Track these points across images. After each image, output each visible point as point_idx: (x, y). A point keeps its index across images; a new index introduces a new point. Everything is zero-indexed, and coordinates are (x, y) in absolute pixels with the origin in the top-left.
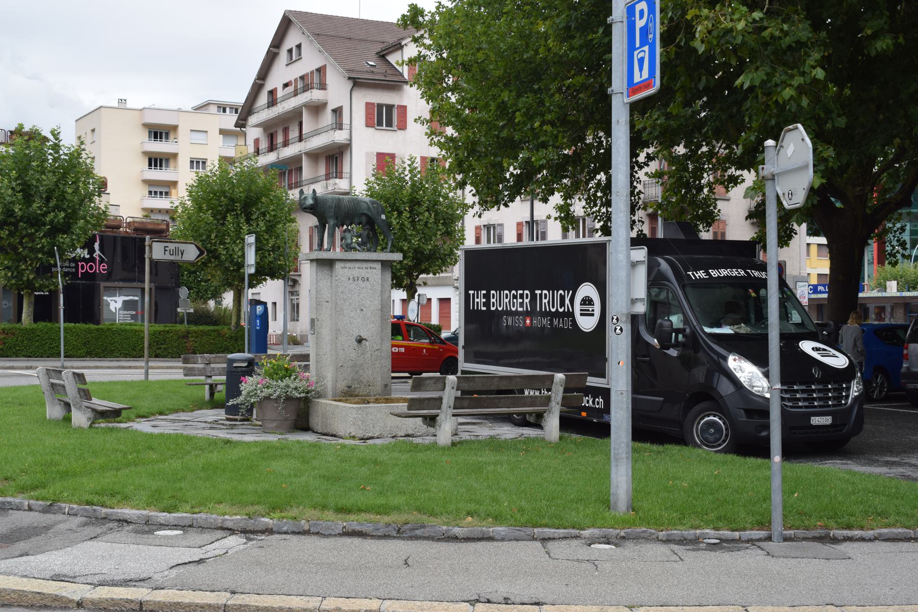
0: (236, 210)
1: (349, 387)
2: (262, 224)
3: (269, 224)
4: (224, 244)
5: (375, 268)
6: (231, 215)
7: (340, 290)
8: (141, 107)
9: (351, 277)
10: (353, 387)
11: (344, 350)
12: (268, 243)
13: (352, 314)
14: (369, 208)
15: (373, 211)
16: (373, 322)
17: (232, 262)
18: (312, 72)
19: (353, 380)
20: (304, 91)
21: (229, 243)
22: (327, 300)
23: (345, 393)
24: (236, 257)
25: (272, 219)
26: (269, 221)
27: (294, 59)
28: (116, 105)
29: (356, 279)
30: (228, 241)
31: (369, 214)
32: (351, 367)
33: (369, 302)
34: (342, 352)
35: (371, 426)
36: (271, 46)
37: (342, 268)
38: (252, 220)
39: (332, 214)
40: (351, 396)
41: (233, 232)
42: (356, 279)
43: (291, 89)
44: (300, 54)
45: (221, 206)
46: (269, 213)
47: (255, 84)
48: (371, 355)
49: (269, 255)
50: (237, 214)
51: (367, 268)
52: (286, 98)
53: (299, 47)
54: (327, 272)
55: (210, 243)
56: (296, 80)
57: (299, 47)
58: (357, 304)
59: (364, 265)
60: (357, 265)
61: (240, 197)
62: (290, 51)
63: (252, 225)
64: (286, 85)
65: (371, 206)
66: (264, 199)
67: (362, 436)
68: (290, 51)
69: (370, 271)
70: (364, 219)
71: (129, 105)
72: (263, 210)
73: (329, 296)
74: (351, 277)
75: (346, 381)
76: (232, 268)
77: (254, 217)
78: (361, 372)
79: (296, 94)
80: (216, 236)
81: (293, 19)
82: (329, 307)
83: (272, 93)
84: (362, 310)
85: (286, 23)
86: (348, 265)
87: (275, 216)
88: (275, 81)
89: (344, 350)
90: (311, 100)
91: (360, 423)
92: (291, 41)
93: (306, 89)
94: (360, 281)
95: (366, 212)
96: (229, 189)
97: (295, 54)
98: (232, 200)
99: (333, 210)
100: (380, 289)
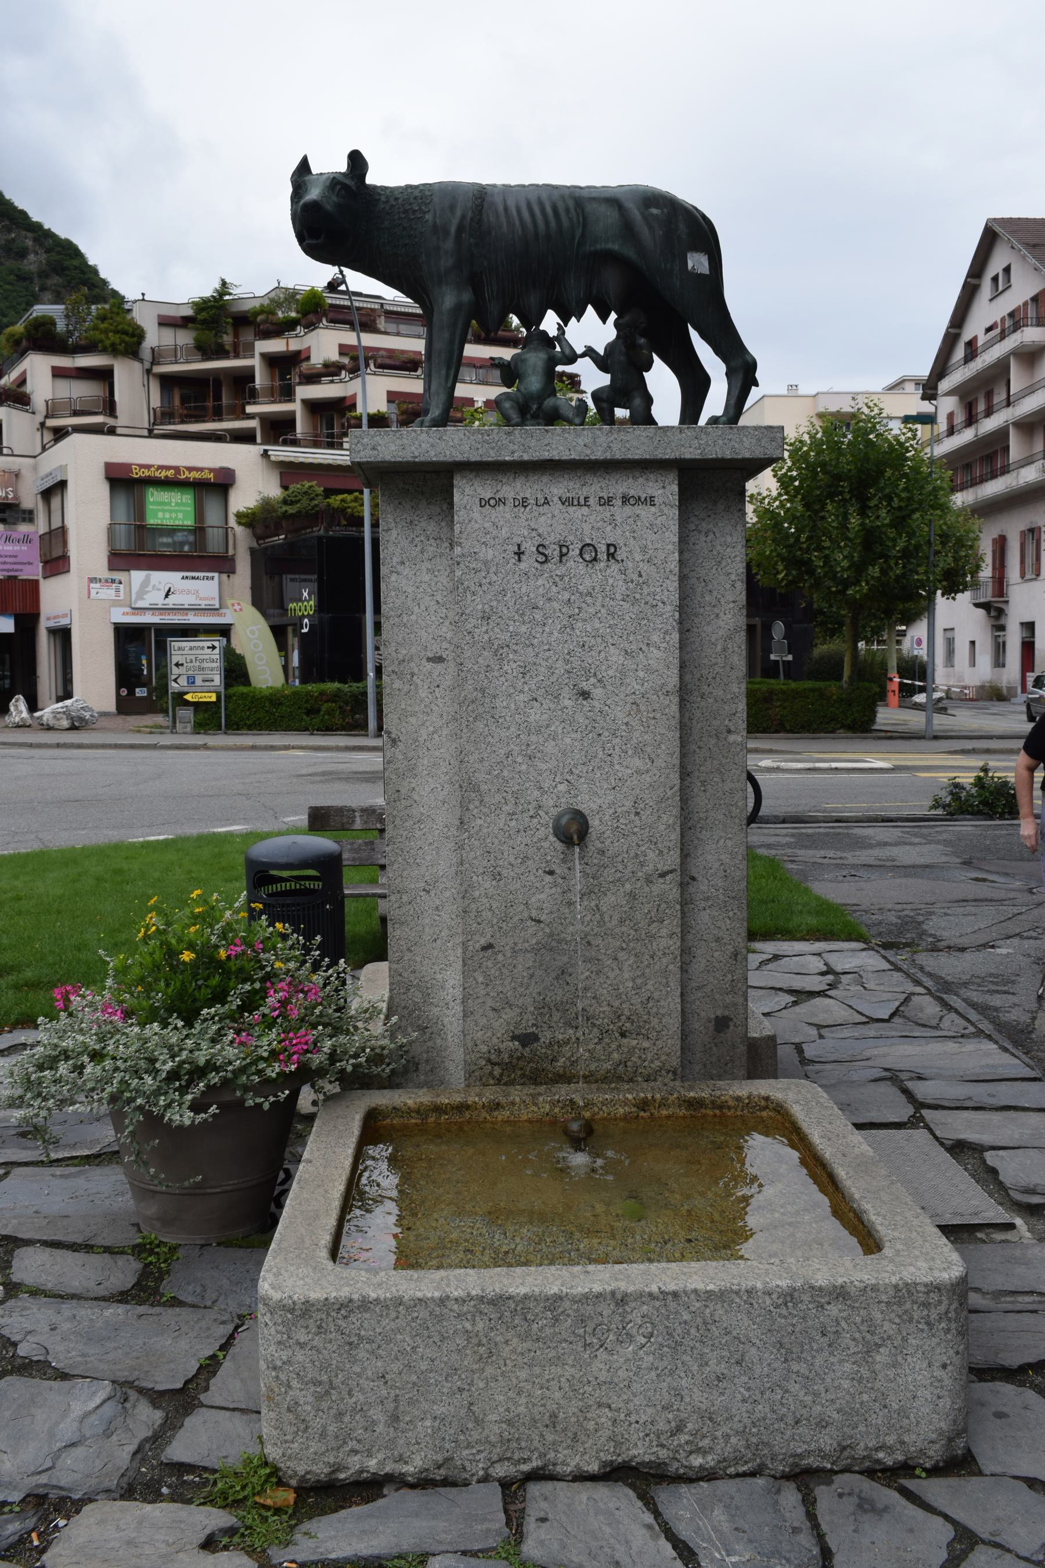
0: (841, 493)
1: (527, 1039)
2: (883, 513)
3: (898, 514)
4: (820, 548)
5: (650, 501)
6: (832, 501)
7: (477, 605)
8: (814, 393)
9: (529, 547)
10: (545, 1036)
11: (497, 876)
12: (894, 546)
13: (535, 715)
14: (627, 228)
15: (645, 233)
16: (639, 750)
17: (834, 578)
18: (1025, 304)
19: (543, 1007)
20: (1014, 331)
21: (829, 548)
22: (435, 649)
23: (509, 1067)
24: (839, 569)
25: (903, 504)
26: (900, 508)
27: (1001, 288)
28: (785, 392)
29: (553, 551)
30: (827, 544)
31: (630, 253)
32: (536, 950)
33: (616, 657)
34: (488, 884)
35: (377, 1414)
36: (968, 276)
37: (483, 503)
38: (870, 507)
39: (446, 262)
40: (535, 1078)
41: (837, 528)
42: (553, 551)
43: (997, 331)
44: (1009, 281)
45: (819, 488)
46: (898, 496)
47: (947, 335)
48: (632, 896)
49: (897, 564)
50: (844, 500)
51: (606, 502)
52: (990, 344)
53: (1007, 270)
54: (432, 528)
55: (800, 549)
56: (1003, 320)
57: (1007, 270)
58: (560, 667)
59: (595, 487)
60: (559, 488)
61: (850, 470)
62: (995, 279)
63: (869, 517)
64: (989, 330)
65: (636, 215)
66: (889, 472)
67: (320, 1470)
68: (995, 279)
69: (621, 512)
70: (612, 281)
71: (801, 392)
72: (887, 491)
73: (446, 630)
74: (529, 547)
75: (509, 1015)
76: (834, 589)
77: (872, 504)
78: (582, 971)
79: (1003, 336)
80: (809, 538)
81: (998, 229)
82: (448, 682)
83: (971, 344)
84: (585, 695)
85: (990, 238)
86: (512, 488)
87: (909, 499)
88: (975, 328)
89: (497, 876)
90: (1022, 345)
91: (306, 1398)
92: (996, 266)
93: (1016, 327)
94: (574, 565)
95: (615, 247)
96: (831, 460)
97: (1003, 282)
98: (838, 477)
99: (449, 244)
100: (675, 598)
